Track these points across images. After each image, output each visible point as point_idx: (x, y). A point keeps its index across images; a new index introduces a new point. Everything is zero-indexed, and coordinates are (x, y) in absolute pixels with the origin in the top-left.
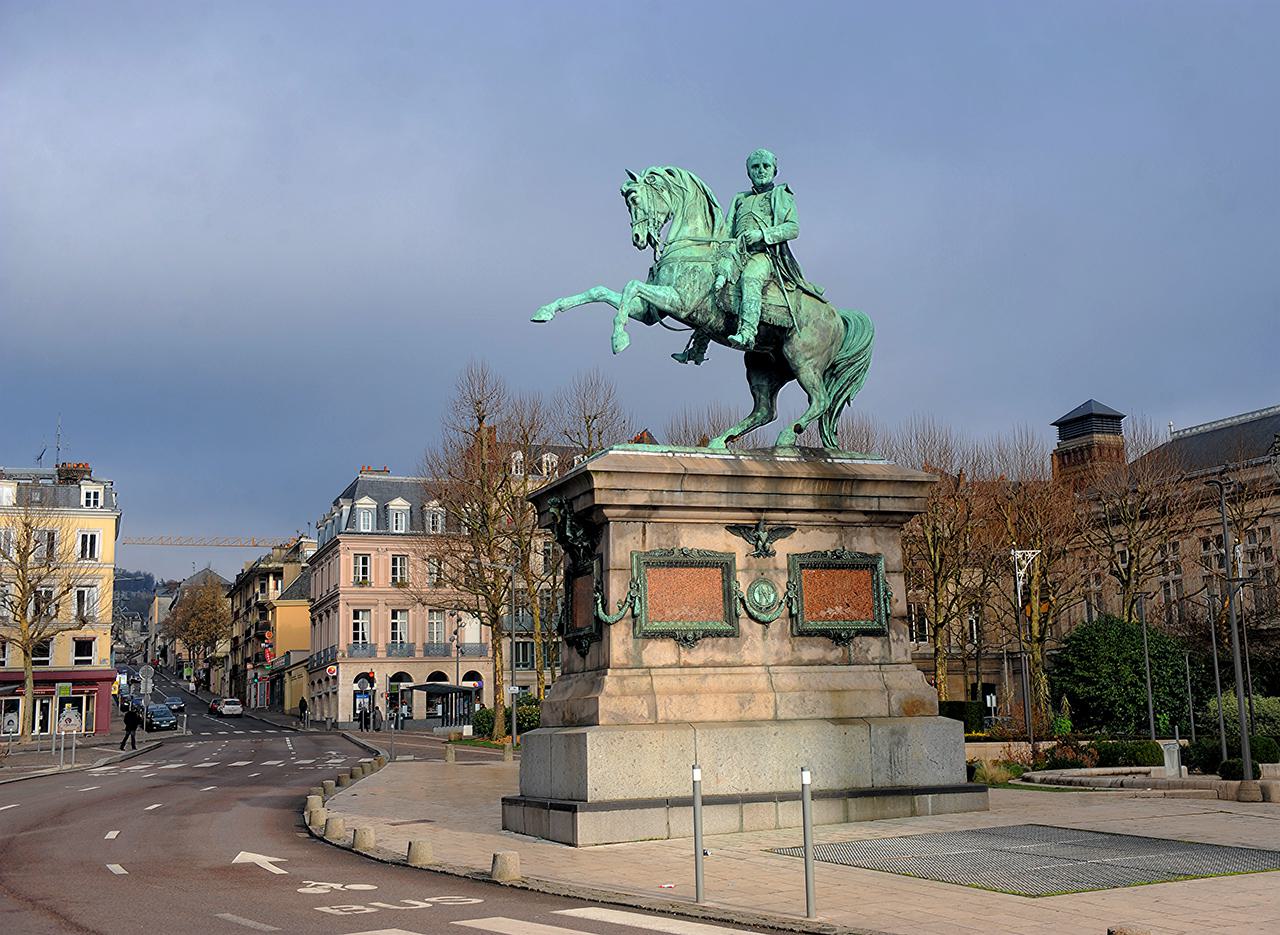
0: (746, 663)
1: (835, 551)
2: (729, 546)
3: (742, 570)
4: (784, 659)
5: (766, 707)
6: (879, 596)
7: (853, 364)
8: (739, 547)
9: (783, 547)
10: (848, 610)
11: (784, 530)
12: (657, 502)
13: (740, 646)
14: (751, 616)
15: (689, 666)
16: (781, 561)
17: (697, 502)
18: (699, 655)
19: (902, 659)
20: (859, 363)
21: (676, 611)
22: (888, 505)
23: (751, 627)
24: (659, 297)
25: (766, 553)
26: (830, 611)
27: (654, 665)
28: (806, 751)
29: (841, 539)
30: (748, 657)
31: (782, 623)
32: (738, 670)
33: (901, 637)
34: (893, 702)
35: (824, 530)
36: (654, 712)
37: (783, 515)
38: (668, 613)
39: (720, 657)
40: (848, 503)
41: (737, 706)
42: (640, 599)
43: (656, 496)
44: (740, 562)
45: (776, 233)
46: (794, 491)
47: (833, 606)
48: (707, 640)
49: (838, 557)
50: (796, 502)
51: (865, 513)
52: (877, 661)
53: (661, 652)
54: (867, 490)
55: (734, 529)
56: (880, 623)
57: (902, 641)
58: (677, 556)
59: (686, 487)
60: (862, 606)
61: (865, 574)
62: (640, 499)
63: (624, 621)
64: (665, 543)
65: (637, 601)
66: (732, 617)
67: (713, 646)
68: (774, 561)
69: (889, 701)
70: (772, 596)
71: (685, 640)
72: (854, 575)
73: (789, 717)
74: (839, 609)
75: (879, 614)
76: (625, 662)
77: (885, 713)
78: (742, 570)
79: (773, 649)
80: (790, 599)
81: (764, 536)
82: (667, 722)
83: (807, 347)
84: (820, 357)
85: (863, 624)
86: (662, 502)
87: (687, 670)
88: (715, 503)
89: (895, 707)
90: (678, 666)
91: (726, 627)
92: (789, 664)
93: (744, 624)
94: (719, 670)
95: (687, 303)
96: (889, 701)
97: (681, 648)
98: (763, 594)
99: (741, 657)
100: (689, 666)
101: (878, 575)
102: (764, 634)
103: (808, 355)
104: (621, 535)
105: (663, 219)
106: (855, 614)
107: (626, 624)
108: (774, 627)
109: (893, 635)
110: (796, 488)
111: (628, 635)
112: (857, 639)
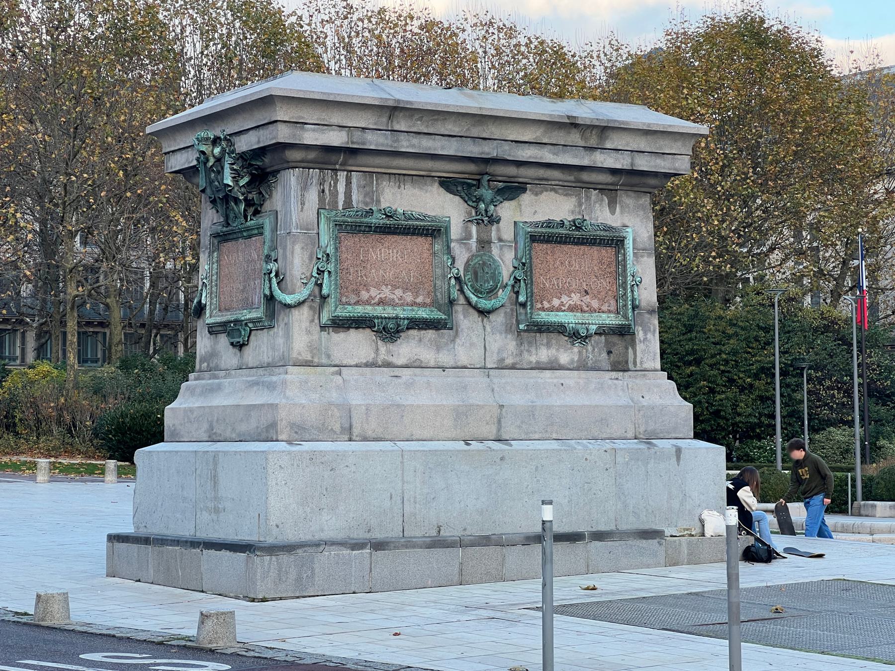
0: (459, 364)
1: (574, 221)
4: (509, 361)
6: (625, 282)
10: (587, 299)
11: (512, 190)
13: (453, 341)
16: (507, 232)
17: (408, 147)
22: (643, 164)
26: (565, 299)
27: (345, 363)
28: (538, 481)
29: (580, 205)
37: (512, 171)
38: (365, 295)
39: (428, 355)
43: (357, 134)
44: (455, 231)
47: (569, 293)
48: (411, 332)
49: (578, 228)
51: (614, 171)
53: (357, 345)
55: (448, 184)
56: (625, 317)
59: (397, 127)
61: (607, 253)
62: (336, 139)
65: (326, 273)
67: (420, 340)
68: (498, 230)
72: (594, 251)
74: (576, 298)
75: (625, 305)
76: (309, 358)
77: (630, 434)
78: (457, 241)
80: (517, 280)
86: (364, 144)
88: (430, 148)
91: (437, 315)
97: (380, 343)
100: (388, 365)
101: (624, 255)
107: (311, 308)
108: (498, 319)
111: (313, 321)
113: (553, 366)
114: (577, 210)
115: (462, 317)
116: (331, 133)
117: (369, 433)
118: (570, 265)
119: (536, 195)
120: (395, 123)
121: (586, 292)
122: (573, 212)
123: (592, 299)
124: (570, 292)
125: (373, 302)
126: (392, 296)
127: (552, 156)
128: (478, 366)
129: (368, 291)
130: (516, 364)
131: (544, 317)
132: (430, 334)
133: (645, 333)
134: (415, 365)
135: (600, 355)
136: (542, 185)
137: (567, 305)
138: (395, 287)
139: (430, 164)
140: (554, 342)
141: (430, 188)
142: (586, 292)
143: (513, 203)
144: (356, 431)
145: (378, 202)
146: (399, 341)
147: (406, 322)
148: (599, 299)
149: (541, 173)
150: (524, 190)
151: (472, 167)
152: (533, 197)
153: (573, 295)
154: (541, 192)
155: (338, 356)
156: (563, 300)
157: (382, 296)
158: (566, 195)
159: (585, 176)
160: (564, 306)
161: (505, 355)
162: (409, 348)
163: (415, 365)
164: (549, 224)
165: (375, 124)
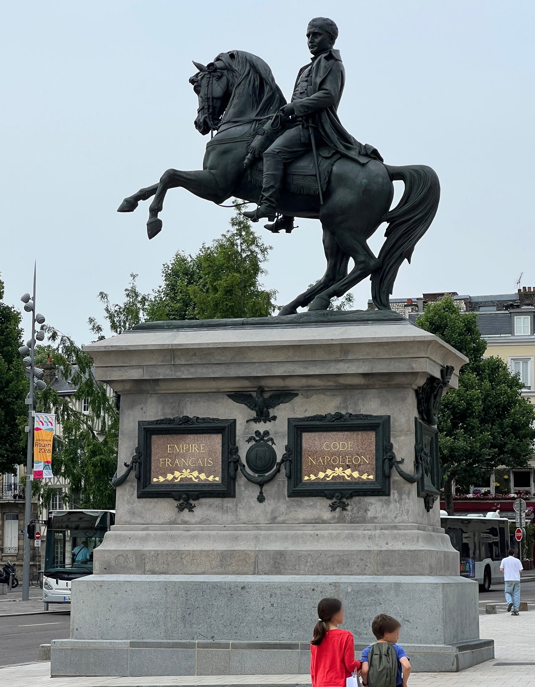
9: (284, 413)
10: (348, 471)
14: (250, 479)
35: (328, 393)
59: (178, 362)
62: (135, 374)
104: (132, 406)
105: (218, 104)
114: (342, 405)
115: (243, 489)
116: (132, 371)
120: (176, 359)
121: (348, 467)
122: (338, 408)
124: (335, 468)
126: (190, 476)
127: (302, 370)
129: (173, 474)
130: (286, 520)
135: (358, 513)
136: (309, 391)
137: (331, 477)
138: (192, 470)
139: (213, 385)
140: (318, 504)
141: (221, 400)
142: (348, 465)
143: (287, 405)
149: (304, 382)
150: (297, 395)
151: (246, 383)
152: (304, 399)
153: (336, 469)
154: (313, 395)
156: (327, 473)
158: (333, 395)
159: (342, 381)
160: (328, 477)
161: (277, 514)
162: (204, 509)
165: (162, 361)
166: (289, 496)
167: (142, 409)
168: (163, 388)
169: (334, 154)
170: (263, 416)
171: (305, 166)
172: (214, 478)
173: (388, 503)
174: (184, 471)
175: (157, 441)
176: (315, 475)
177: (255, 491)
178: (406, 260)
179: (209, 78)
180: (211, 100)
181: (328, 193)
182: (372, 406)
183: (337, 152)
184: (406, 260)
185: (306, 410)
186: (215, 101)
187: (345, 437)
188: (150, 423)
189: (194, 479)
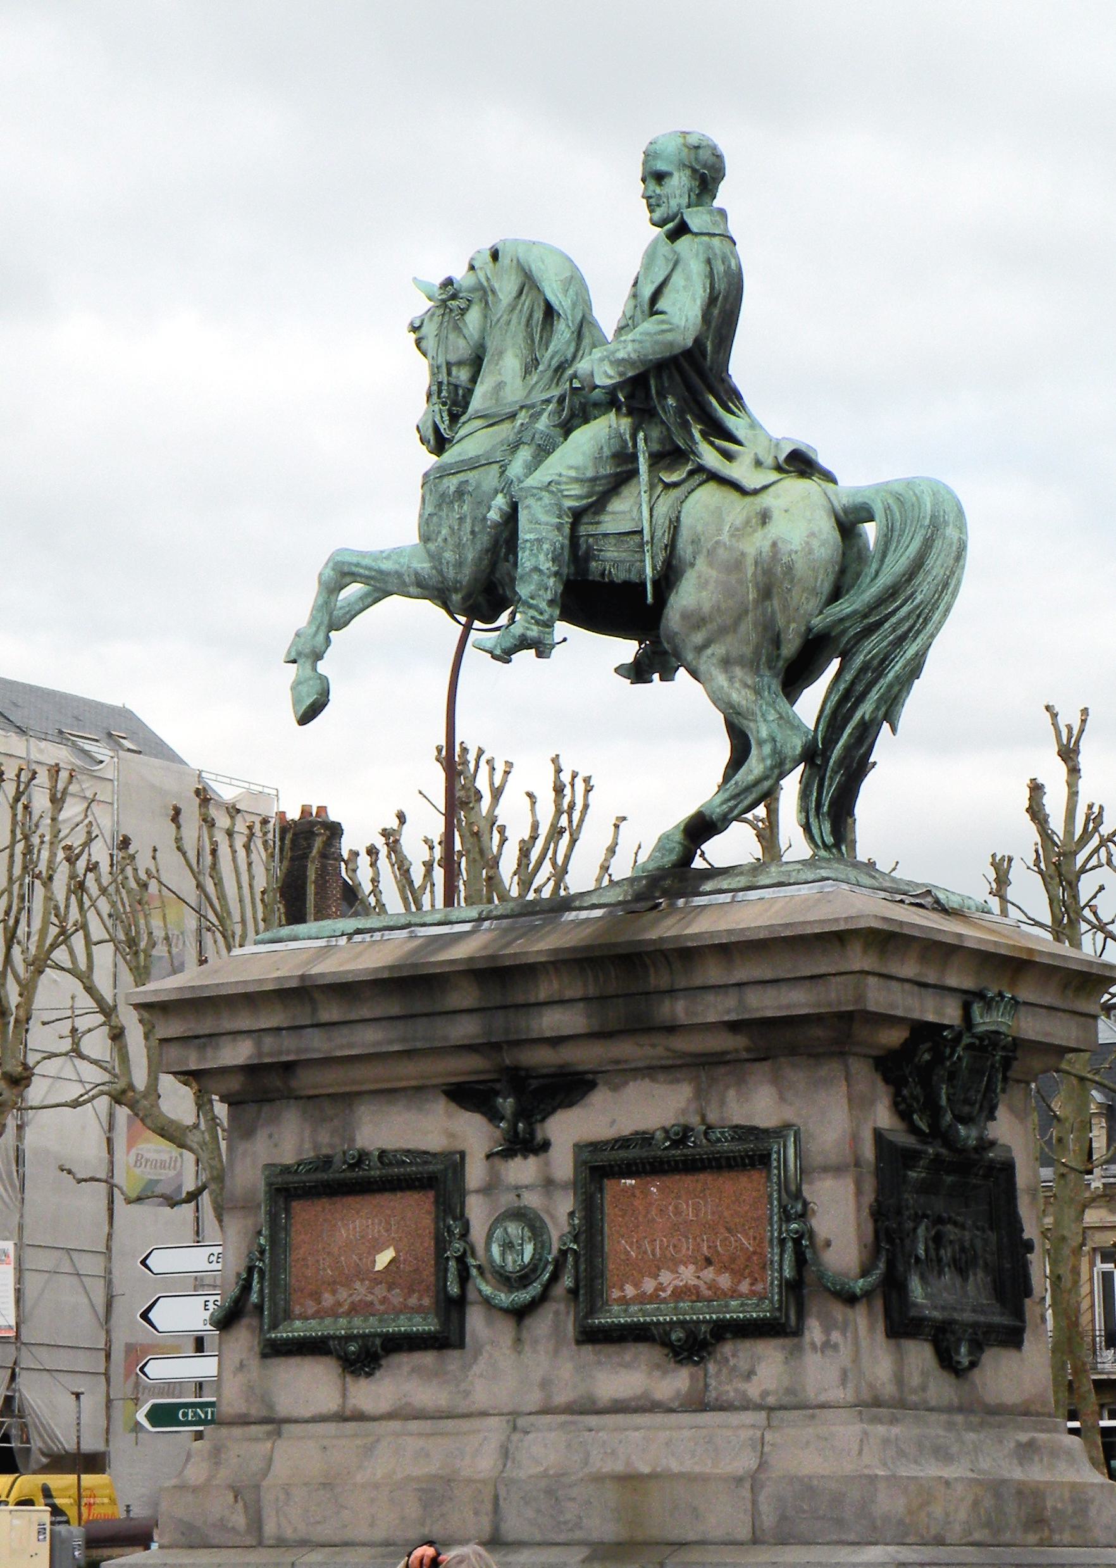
0: (475, 1408)
2: (451, 1135)
3: (477, 1191)
4: (561, 1398)
5: (476, 1513)
7: (879, 624)
8: (471, 1134)
9: (568, 1130)
10: (709, 1274)
11: (571, 1087)
12: (271, 1055)
13: (466, 1368)
15: (360, 1417)
16: (562, 1163)
18: (375, 1393)
19: (836, 1394)
20: (894, 620)
21: (343, 1294)
23: (489, 1322)
24: (388, 574)
25: (537, 1147)
30: (482, 1394)
31: (557, 1313)
32: (449, 1424)
33: (836, 1336)
34: (764, 1508)
36: (256, 1523)
38: (328, 1299)
40: (679, 1010)
41: (413, 1509)
42: (262, 1272)
43: (269, 1042)
44: (475, 1173)
45: (621, 355)
46: (542, 996)
47: (673, 1264)
49: (676, 1144)
50: (553, 1022)
52: (771, 1400)
53: (310, 1385)
54: (713, 973)
55: (466, 1095)
57: (835, 1347)
58: (338, 1172)
59: (325, 1016)
60: (741, 1261)
63: (245, 1321)
64: (326, 1141)
66: (453, 1308)
69: (754, 1503)
70: (529, 1249)
71: (363, 1357)
73: (525, 1537)
74: (687, 1274)
76: (244, 1410)
77: (744, 1533)
78: (477, 1191)
79: (537, 1375)
81: (507, 1104)
82: (281, 1543)
83: (696, 620)
84: (729, 639)
85: (735, 1311)
87: (351, 1427)
89: (768, 1519)
90: (341, 1417)
92: (570, 1409)
93: (476, 1321)
94: (413, 1425)
95: (451, 573)
96: (754, 1503)
97: (349, 1379)
98: (507, 1245)
99: (467, 1394)
102: (518, 1341)
103: (698, 638)
106: (725, 1281)
107: (249, 1327)
108: (542, 1324)
109: (814, 1331)
110: (544, 990)
112: (727, 1348)
113: (646, 1406)
117: (289, 1533)
118: (678, 1212)
119: (615, 1088)
121: (709, 1262)
123: (719, 1272)
125: (341, 1310)
126: (369, 1298)
128: (505, 1411)
129: (334, 1292)
131: (614, 1316)
132: (427, 1358)
133: (827, 1331)
134: (402, 1414)
144: (270, 1528)
145: (352, 1140)
146: (378, 1374)
147: (378, 1341)
148: (733, 1272)
153: (682, 1269)
154: (626, 1083)
155: (285, 1405)
156: (661, 1279)
157: (356, 1298)
158: (672, 1082)
160: (664, 1290)
163: (402, 1414)
164: (623, 1142)
166: (579, 1342)
167: (270, 1136)
168: (306, 1081)
169: (691, 473)
170: (523, 1143)
171: (629, 510)
172: (419, 1299)
173: (796, 1352)
174: (358, 1285)
175: (304, 1212)
176: (636, 1285)
177: (505, 1329)
178: (886, 726)
179: (443, 315)
180: (444, 370)
181: (669, 576)
182: (758, 1104)
183: (700, 469)
184: (886, 726)
185: (613, 1122)
186: (454, 370)
187: (699, 1185)
188: (286, 1169)
189: (376, 1302)
